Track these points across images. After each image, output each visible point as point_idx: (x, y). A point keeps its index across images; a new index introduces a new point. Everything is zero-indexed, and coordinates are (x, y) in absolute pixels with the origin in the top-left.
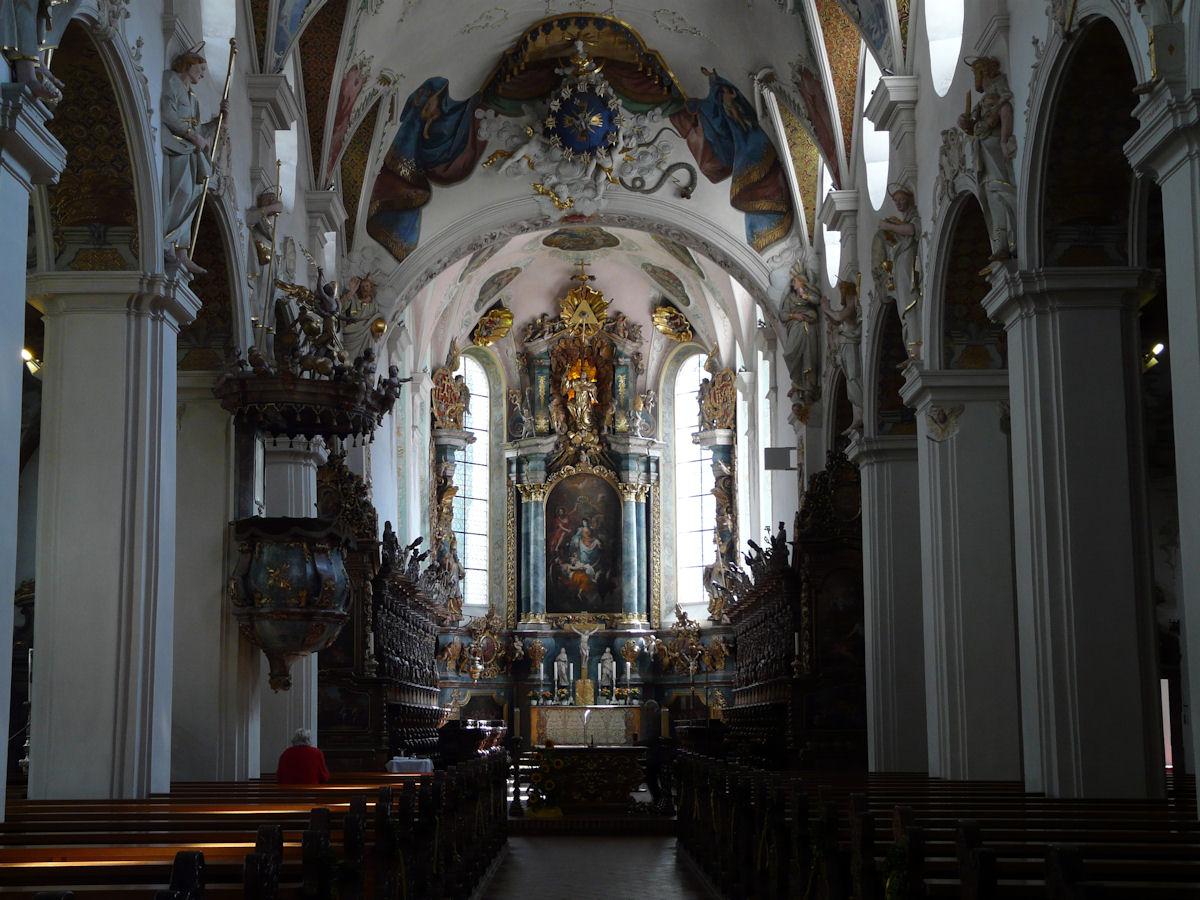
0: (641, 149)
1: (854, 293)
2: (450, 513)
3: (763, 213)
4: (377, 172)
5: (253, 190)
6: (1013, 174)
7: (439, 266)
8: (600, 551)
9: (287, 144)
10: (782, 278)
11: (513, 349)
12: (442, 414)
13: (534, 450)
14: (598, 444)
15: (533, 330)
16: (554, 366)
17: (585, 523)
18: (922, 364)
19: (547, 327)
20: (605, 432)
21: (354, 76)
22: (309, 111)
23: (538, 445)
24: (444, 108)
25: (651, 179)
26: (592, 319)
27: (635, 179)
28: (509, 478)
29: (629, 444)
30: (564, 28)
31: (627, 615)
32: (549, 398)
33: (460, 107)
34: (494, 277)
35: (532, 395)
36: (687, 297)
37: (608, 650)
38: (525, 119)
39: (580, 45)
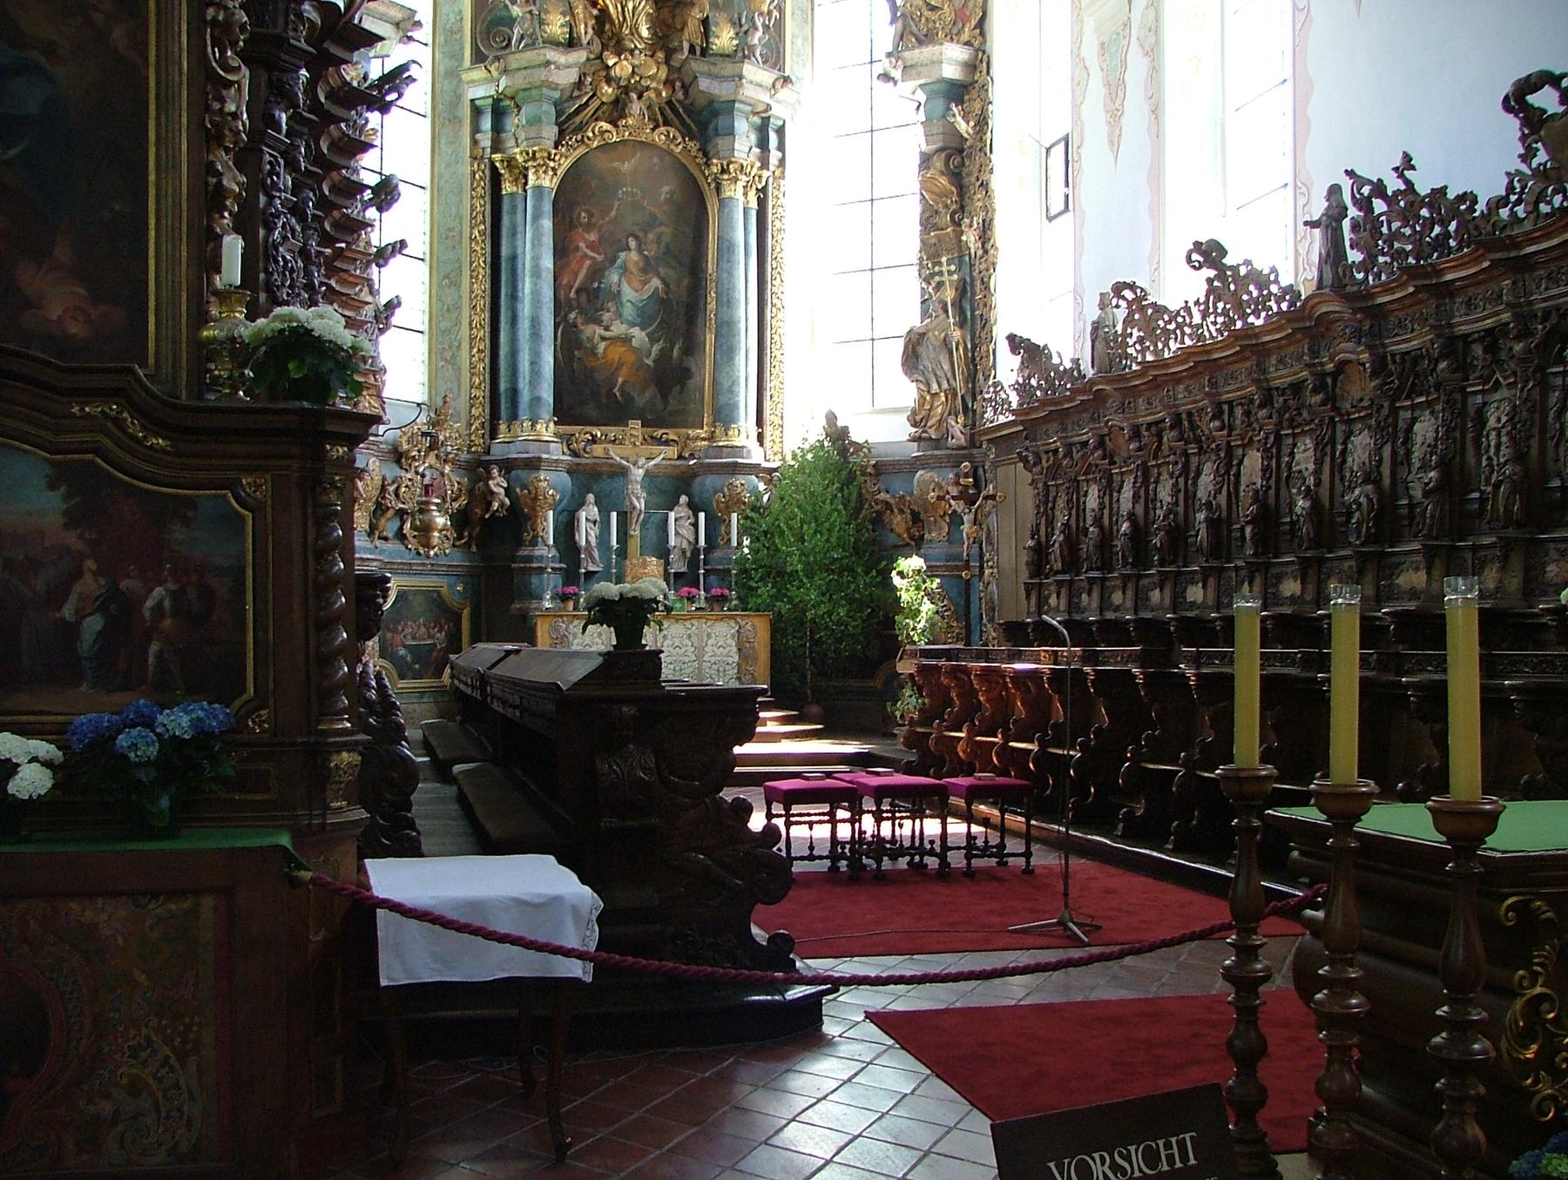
8: (663, 301)
13: (542, 74)
17: (632, 243)
23: (548, 63)
29: (741, 77)
31: (727, 429)
37: (684, 499)
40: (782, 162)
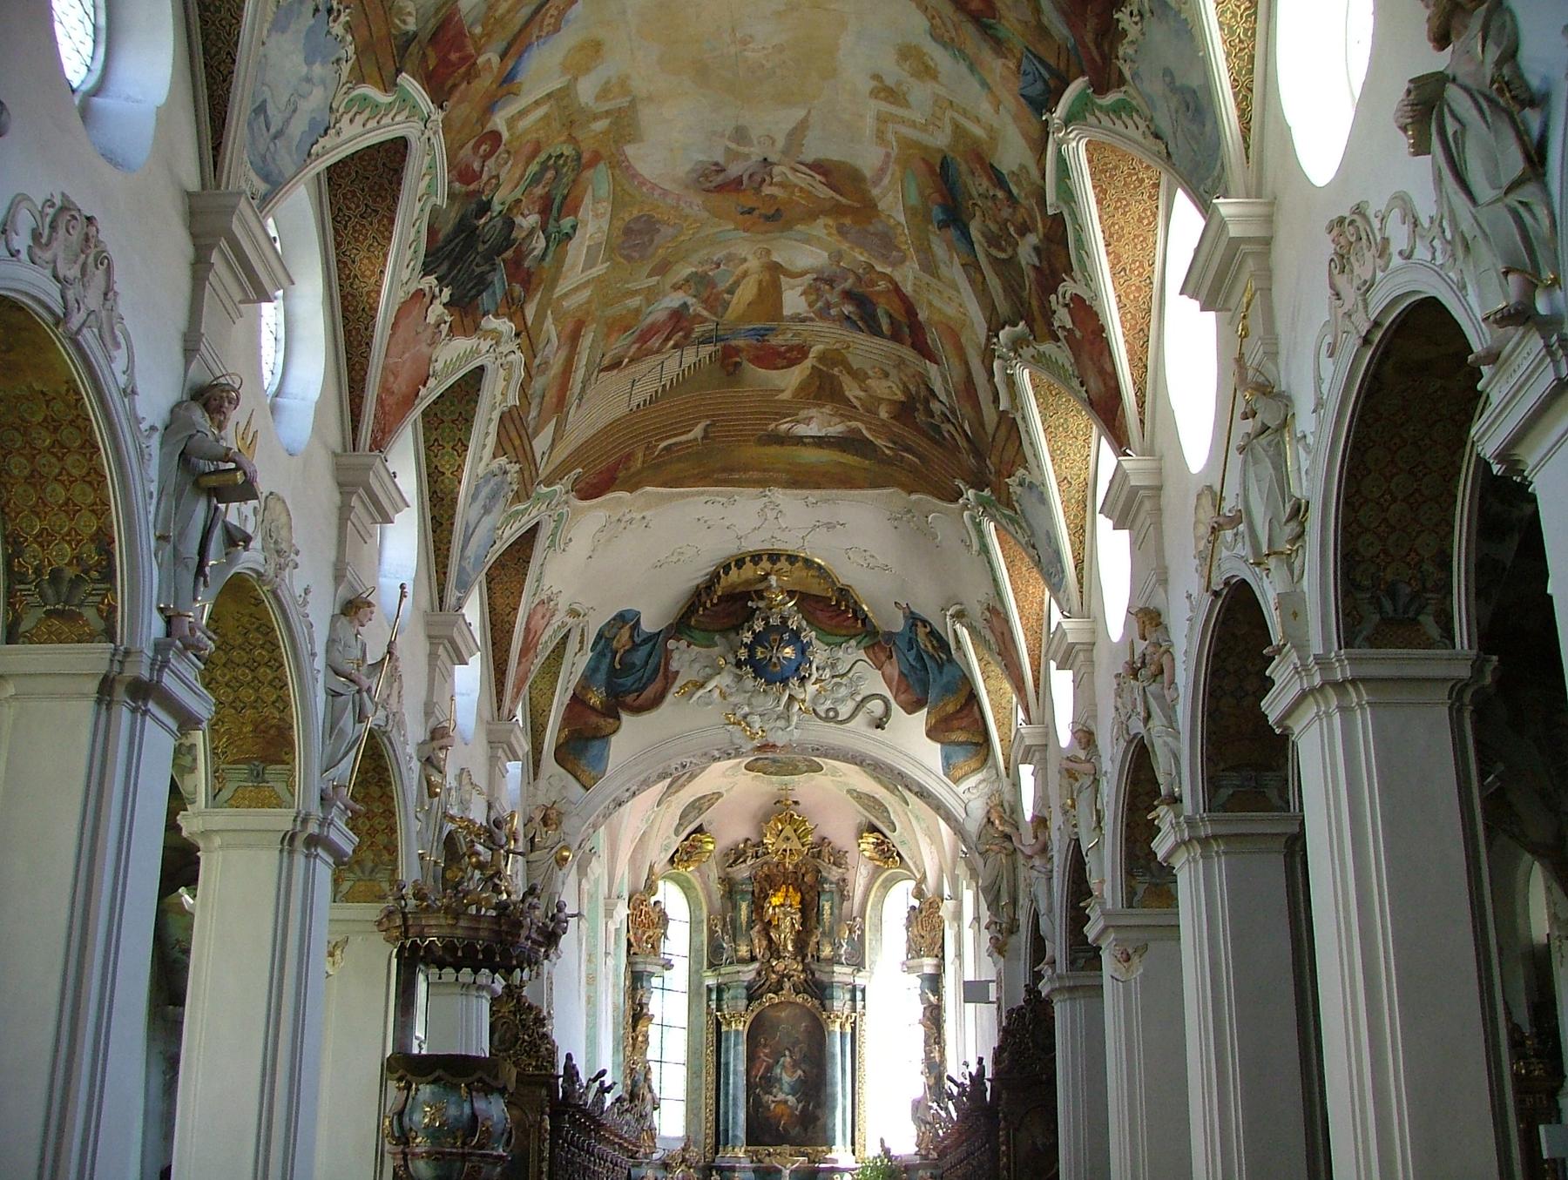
0: (835, 680)
1: (1046, 827)
2: (646, 1041)
3: (960, 744)
4: (567, 700)
5: (426, 723)
6: (1177, 721)
7: (628, 794)
9: (469, 678)
10: (978, 808)
11: (714, 873)
12: (639, 940)
13: (736, 977)
14: (803, 971)
15: (736, 855)
16: (757, 891)
18: (1105, 903)
19: (750, 852)
20: (809, 959)
21: (541, 610)
22: (494, 644)
24: (636, 639)
25: (845, 710)
26: (796, 845)
27: (828, 710)
28: (709, 1006)
30: (756, 564)
32: (751, 924)
33: (652, 638)
34: (695, 801)
35: (733, 920)
36: (893, 823)
38: (716, 649)
39: (773, 579)
40: (864, 1007)
